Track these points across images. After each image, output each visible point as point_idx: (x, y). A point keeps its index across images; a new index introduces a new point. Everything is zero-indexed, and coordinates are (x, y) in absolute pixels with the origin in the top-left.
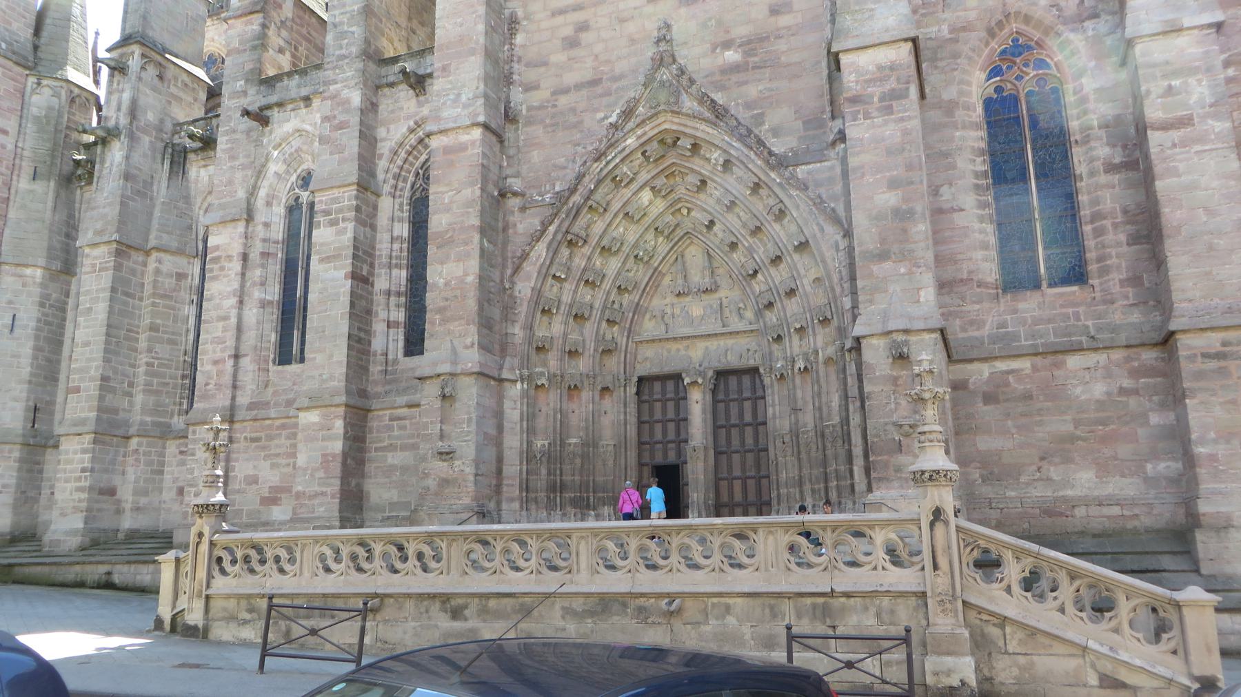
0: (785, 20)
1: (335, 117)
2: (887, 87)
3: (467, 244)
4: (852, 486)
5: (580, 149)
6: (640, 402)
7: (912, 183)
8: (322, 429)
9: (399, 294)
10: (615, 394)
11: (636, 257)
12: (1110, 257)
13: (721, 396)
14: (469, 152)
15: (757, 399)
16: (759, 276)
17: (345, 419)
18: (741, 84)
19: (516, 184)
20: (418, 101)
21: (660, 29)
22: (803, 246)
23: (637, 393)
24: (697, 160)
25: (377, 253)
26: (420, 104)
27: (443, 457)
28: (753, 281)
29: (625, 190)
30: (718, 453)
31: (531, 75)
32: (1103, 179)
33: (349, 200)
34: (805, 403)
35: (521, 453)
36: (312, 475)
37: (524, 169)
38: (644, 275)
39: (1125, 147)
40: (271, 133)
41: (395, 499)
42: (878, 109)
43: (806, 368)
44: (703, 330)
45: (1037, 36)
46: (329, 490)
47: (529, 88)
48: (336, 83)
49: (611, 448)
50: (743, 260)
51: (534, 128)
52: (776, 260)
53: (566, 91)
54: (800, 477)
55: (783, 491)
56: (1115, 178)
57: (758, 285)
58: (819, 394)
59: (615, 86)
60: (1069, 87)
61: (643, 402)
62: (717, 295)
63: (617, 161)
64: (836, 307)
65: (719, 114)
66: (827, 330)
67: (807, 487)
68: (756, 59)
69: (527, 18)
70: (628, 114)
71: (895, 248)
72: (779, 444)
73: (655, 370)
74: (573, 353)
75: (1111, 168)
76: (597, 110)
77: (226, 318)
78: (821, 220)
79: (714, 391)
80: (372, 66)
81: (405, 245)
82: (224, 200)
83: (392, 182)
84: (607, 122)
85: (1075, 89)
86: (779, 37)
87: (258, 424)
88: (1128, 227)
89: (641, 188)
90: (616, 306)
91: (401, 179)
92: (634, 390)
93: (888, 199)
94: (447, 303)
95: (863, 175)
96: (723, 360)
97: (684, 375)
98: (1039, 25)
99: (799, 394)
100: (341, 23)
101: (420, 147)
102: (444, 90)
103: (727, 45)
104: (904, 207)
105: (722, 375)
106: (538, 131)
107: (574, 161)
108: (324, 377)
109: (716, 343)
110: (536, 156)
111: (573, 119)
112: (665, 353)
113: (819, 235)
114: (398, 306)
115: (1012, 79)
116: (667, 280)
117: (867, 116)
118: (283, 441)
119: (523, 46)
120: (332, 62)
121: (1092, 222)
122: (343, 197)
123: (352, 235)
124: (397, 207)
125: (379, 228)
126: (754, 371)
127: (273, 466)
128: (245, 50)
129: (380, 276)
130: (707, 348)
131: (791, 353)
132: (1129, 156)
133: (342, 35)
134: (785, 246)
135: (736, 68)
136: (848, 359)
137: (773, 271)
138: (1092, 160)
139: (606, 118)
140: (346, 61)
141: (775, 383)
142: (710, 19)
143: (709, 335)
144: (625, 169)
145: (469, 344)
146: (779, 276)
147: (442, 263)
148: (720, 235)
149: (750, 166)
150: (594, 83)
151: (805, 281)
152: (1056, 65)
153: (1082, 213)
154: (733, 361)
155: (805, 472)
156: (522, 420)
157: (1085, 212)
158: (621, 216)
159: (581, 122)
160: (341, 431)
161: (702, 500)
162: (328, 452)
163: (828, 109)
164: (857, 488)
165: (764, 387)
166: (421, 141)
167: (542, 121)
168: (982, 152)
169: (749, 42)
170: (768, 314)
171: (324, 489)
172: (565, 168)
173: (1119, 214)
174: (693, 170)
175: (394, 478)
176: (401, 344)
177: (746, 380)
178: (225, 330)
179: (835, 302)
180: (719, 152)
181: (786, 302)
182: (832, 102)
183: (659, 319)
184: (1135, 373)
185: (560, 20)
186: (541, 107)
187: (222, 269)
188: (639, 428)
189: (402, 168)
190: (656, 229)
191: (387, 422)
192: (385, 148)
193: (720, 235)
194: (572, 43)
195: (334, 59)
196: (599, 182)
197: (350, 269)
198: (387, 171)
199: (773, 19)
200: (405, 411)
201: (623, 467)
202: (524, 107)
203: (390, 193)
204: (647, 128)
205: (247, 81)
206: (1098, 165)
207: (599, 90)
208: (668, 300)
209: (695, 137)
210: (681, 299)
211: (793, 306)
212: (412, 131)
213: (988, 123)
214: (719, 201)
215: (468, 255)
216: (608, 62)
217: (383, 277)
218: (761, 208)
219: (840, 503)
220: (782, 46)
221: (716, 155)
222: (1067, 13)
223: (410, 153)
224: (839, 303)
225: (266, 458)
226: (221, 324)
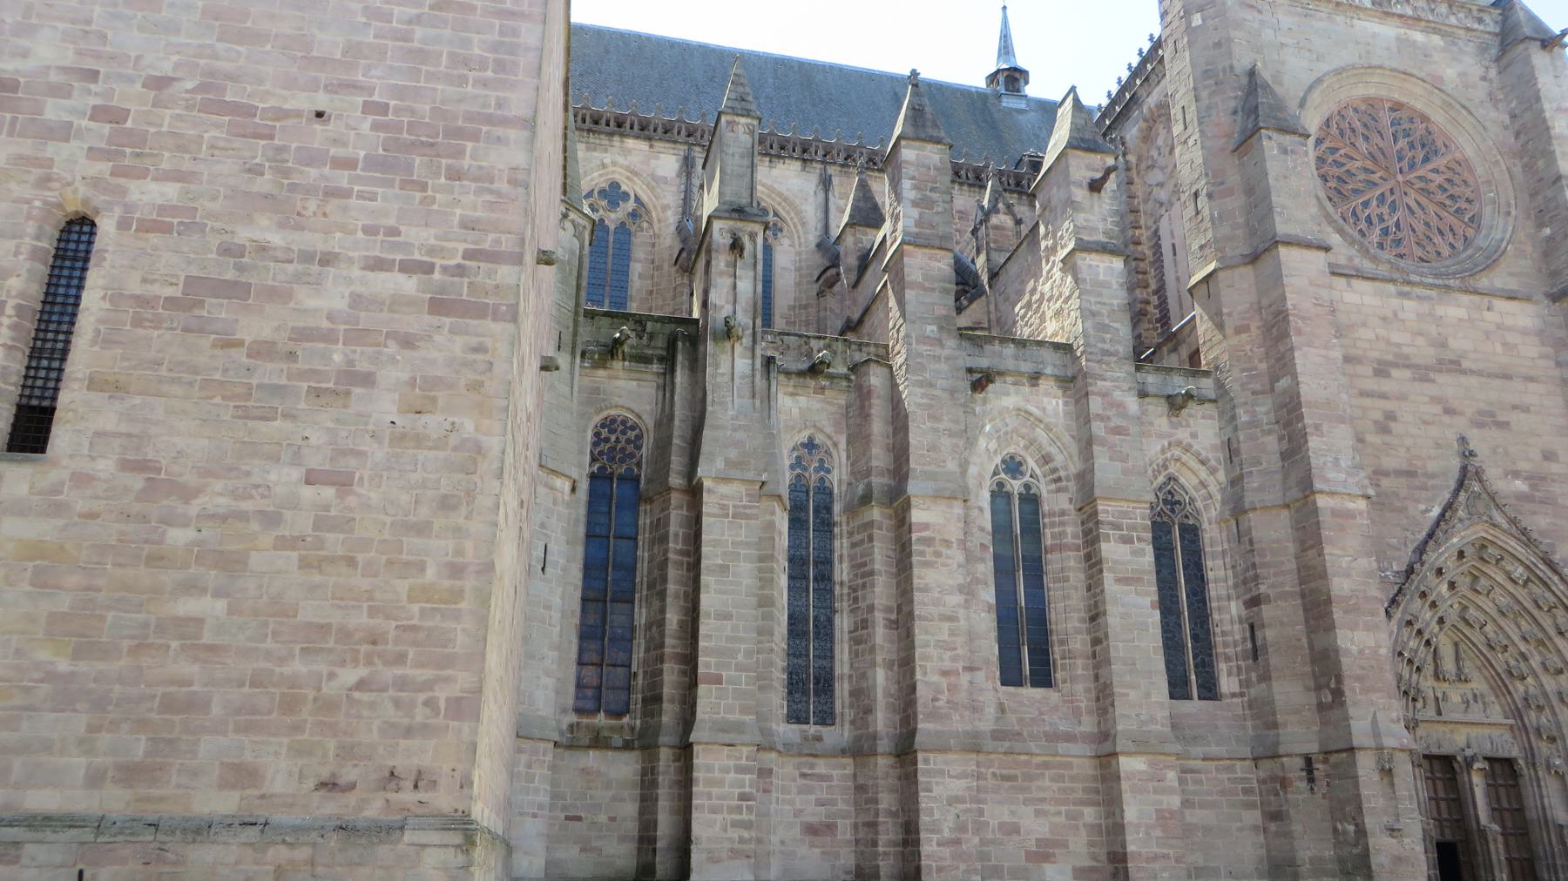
0: (1555, 468)
5: (1408, 534)
8: (1152, 780)
14: (1359, 521)
18: (1534, 513)
26: (1174, 426)
36: (1147, 833)
40: (985, 401)
41: (1201, 863)
46: (1171, 852)
48: (1105, 380)
59: (1430, 483)
65: (1525, 537)
76: (1418, 501)
77: (951, 619)
82: (929, 468)
86: (1553, 481)
87: (1010, 758)
103: (1516, 474)
107: (1405, 545)
108: (1142, 717)
118: (1047, 783)
127: (1038, 813)
128: (933, 290)
139: (1427, 511)
149: (1554, 588)
159: (1406, 508)
162: (1165, 807)
171: (1165, 851)
172: (1399, 549)
178: (952, 633)
185: (1367, 402)
187: (938, 554)
199: (1546, 464)
200: (1199, 764)
205: (941, 328)
207: (1417, 482)
225: (1026, 802)
226: (946, 625)
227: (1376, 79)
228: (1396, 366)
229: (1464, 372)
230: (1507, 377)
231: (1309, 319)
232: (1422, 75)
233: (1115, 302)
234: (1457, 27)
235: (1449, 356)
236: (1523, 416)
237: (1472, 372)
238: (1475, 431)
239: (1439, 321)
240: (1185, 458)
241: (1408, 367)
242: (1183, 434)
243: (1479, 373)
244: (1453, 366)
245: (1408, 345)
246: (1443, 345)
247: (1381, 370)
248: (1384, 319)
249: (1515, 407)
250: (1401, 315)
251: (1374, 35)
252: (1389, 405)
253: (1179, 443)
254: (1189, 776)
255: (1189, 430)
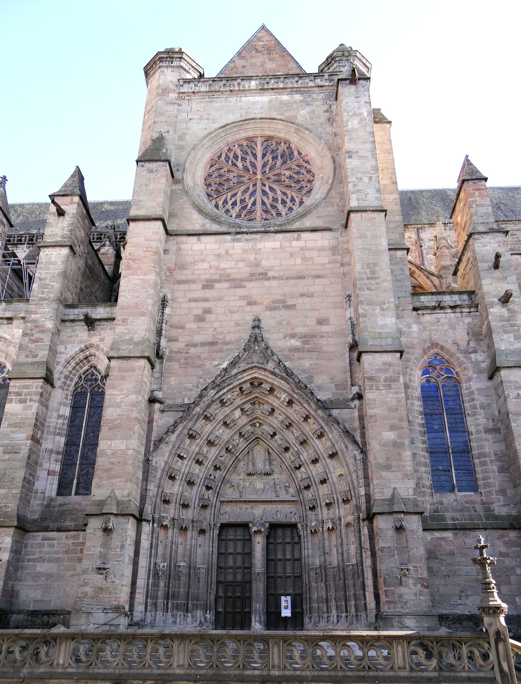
0: (325, 328)
1: (33, 335)
2: (388, 375)
3: (130, 430)
4: (365, 604)
5: (201, 380)
6: (220, 540)
7: (403, 428)
9: (58, 453)
10: (207, 534)
11: (227, 449)
12: (490, 478)
13: (272, 540)
15: (294, 543)
16: (302, 469)
17: (13, 537)
18: (300, 359)
19: (159, 395)
20: (89, 334)
21: (254, 320)
22: (333, 456)
23: (219, 535)
24: (271, 397)
25: (47, 424)
26: (90, 336)
27: (100, 572)
28: (297, 471)
29: (226, 408)
30: (268, 578)
31: (174, 333)
32: (484, 436)
33: (37, 388)
34: (331, 549)
35: (149, 570)
37: (165, 387)
38: (230, 460)
39: (493, 420)
41: (39, 598)
42: (383, 385)
43: (333, 528)
44: (263, 498)
45: (447, 357)
47: (170, 340)
49: (203, 571)
50: (293, 458)
51: (173, 363)
52: (315, 461)
53: (195, 345)
54: (327, 597)
55: (315, 605)
56: (490, 436)
57: (300, 474)
58: (342, 545)
59: (225, 348)
60: (464, 385)
61: (222, 540)
62: (272, 477)
63: (225, 391)
64: (354, 492)
65: (288, 374)
66: (348, 506)
67: (333, 603)
68: (309, 346)
69: (173, 300)
70: (233, 364)
71: (395, 463)
72: (312, 574)
73: (232, 520)
74: (185, 506)
75: (488, 431)
76: (214, 359)
78: (346, 441)
79: (268, 537)
80: (61, 307)
81: (66, 422)
83: (63, 380)
84: (222, 367)
85: (466, 386)
88: (498, 462)
89: (236, 408)
90: (212, 477)
91: (69, 379)
92: (216, 532)
93: (391, 435)
94: (111, 466)
95: (376, 421)
96: (275, 518)
97: (250, 525)
98: (448, 352)
99: (327, 543)
100: (45, 279)
101: (85, 361)
102: (122, 333)
103: (293, 336)
104: (399, 441)
105: (274, 527)
106: (175, 365)
109: (270, 506)
110: (173, 381)
111: (199, 363)
112: (238, 510)
113: (345, 450)
114: (56, 461)
115: (435, 377)
116: (242, 464)
117: (377, 389)
119: (170, 315)
120: (35, 300)
121: (479, 458)
122: (32, 386)
123: (35, 411)
124: (64, 396)
125: (50, 408)
126: (294, 526)
129: (47, 439)
130: (265, 509)
131: (322, 517)
132: (495, 425)
133: (45, 286)
134: (322, 453)
135: (297, 350)
136: (362, 525)
137: (312, 467)
138: (478, 425)
139: (219, 365)
140: (46, 302)
141: (309, 535)
142: (283, 320)
143: (267, 501)
144: (229, 396)
145: (126, 495)
146: (316, 471)
147: (111, 440)
148: (279, 442)
150: (213, 343)
151: (333, 475)
152: (456, 373)
153: (473, 452)
154: (281, 518)
155: (332, 594)
156: (151, 548)
157: (475, 452)
158: (222, 423)
160: (9, 546)
161: (261, 609)
163: (349, 380)
164: (368, 606)
165: (299, 537)
166: (86, 358)
167: (179, 360)
168: (421, 413)
169: (305, 336)
170: (306, 492)
172: (191, 390)
173: (493, 456)
174: (267, 402)
175: (40, 583)
176: (55, 487)
177: (288, 532)
179: (354, 490)
180: (286, 394)
181: (320, 487)
182: (351, 377)
183: (236, 488)
184: (507, 544)
185: (193, 304)
186: (178, 352)
188: (218, 556)
189: (71, 372)
190: (240, 433)
191: (40, 541)
192: (62, 359)
193: (279, 442)
194: (200, 319)
195: (37, 299)
196: (213, 401)
197: (31, 433)
198: (61, 373)
199: (318, 327)
201: (209, 582)
202: (168, 350)
203: (61, 387)
204: (245, 375)
206: (481, 428)
207: (216, 348)
208: (241, 477)
209: (273, 384)
210: (250, 477)
211: (324, 489)
212: (82, 351)
213: (423, 397)
214: (282, 422)
215: (130, 437)
216: (221, 333)
217: (49, 441)
218: (308, 429)
219: (357, 615)
220: (323, 341)
221: (284, 396)
222: (462, 348)
223: (77, 364)
224: (356, 491)
227: (251, 126)
228: (219, 281)
229: (269, 279)
230: (301, 277)
231: (139, 260)
232: (283, 117)
233: (56, 272)
234: (314, 87)
235: (260, 270)
236: (306, 300)
237: (274, 278)
238: (268, 313)
239: (258, 252)
240: (97, 353)
241: (228, 281)
242: (95, 340)
243: (280, 278)
244: (264, 276)
245: (230, 268)
246: (258, 265)
247: (208, 285)
248: (218, 256)
249: (302, 295)
250: (230, 252)
251: (254, 103)
252: (206, 305)
253: (91, 346)
254: (46, 542)
255: (99, 337)
